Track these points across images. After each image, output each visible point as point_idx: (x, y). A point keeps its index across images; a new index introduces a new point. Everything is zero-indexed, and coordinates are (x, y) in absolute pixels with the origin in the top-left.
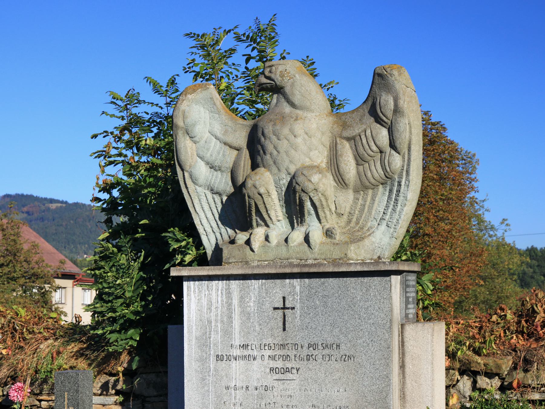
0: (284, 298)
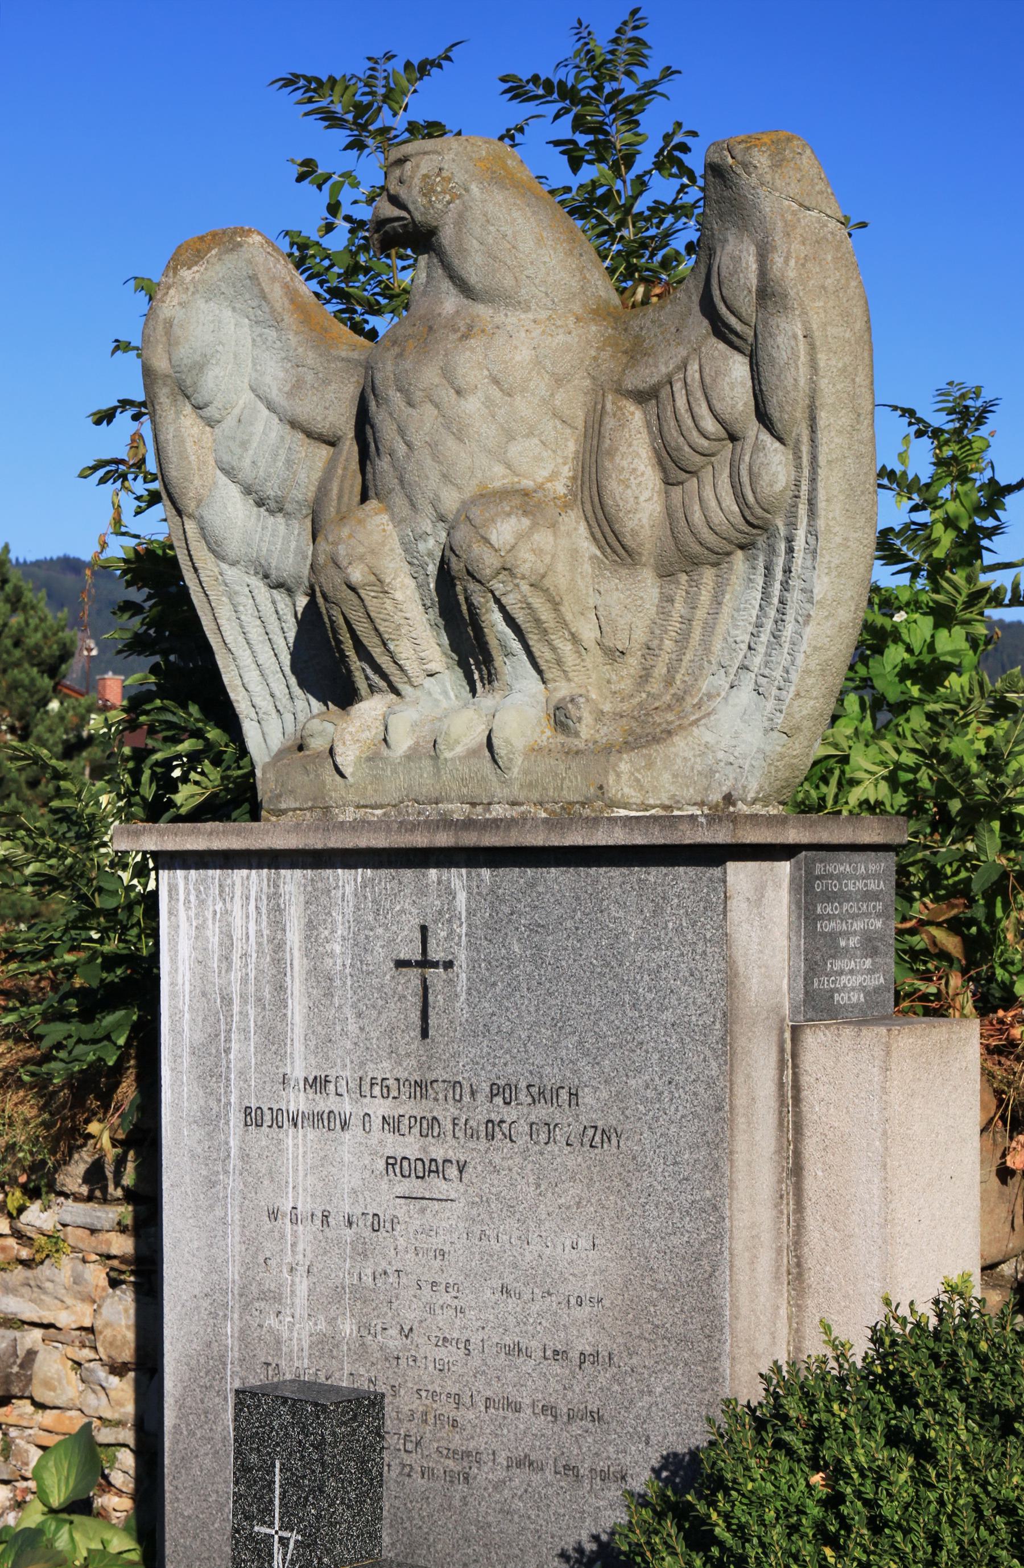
0: (424, 929)
